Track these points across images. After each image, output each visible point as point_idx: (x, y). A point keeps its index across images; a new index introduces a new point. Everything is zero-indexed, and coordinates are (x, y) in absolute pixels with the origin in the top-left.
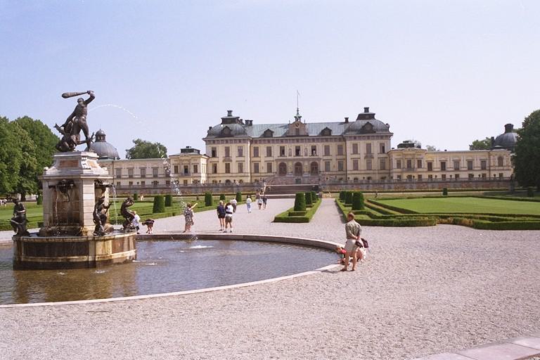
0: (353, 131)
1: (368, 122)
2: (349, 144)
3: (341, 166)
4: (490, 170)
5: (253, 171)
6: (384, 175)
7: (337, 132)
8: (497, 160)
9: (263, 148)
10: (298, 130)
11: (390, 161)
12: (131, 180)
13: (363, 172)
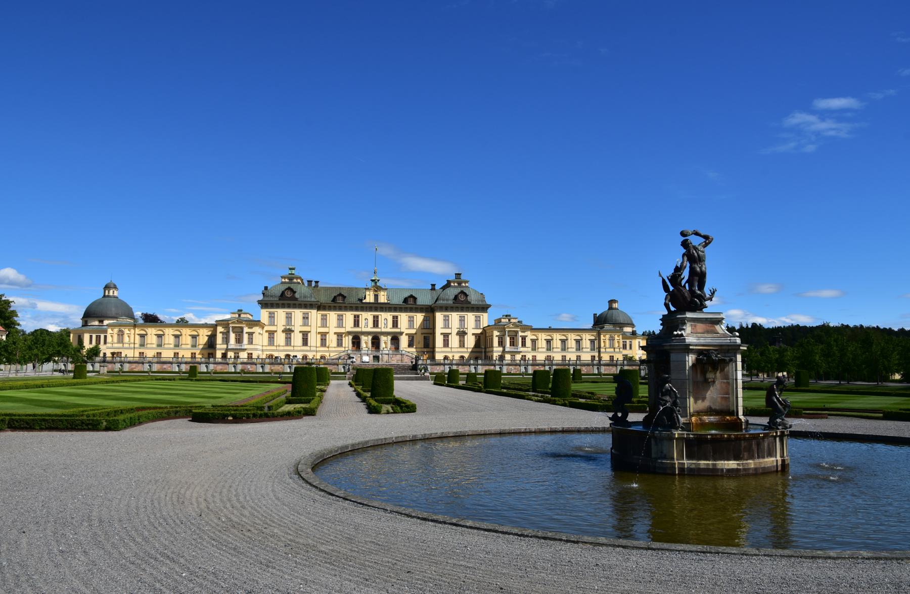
0: (443, 300)
1: (462, 292)
2: (439, 316)
4: (599, 352)
5: (319, 344)
6: (478, 354)
7: (425, 299)
8: (607, 342)
9: (332, 316)
10: (376, 297)
12: (159, 351)
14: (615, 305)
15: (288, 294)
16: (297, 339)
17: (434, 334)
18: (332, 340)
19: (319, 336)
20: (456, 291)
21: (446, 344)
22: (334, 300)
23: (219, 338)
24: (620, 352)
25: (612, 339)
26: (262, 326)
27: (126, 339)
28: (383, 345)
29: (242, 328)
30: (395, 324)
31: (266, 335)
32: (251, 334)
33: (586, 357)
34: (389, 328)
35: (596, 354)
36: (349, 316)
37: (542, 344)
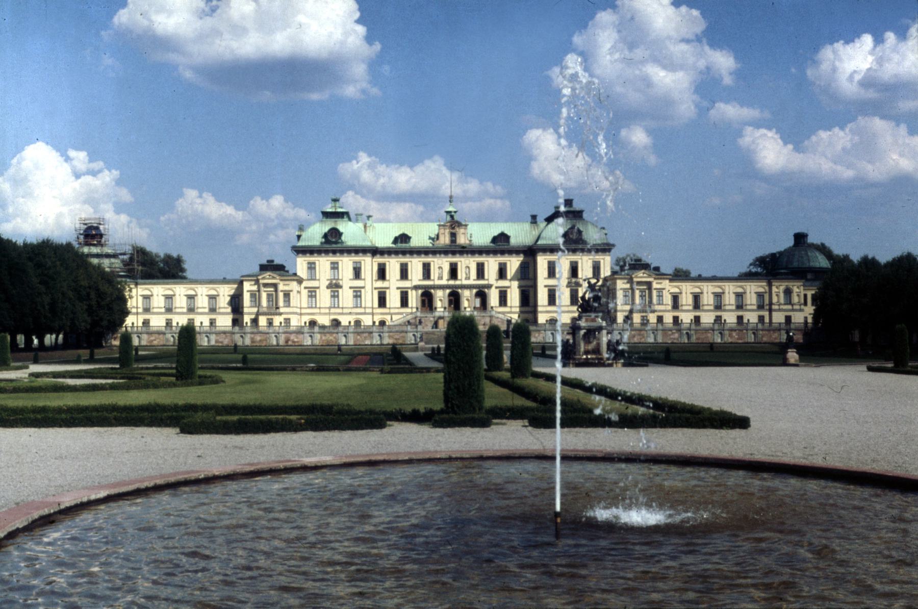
2: (542, 262)
3: (528, 299)
4: (770, 311)
5: (376, 304)
8: (782, 295)
9: (393, 265)
11: (611, 293)
13: (566, 309)
17: (535, 286)
19: (376, 293)
21: (552, 300)
23: (247, 297)
24: (801, 310)
25: (788, 292)
26: (300, 281)
29: (275, 286)
30: (481, 273)
31: (305, 293)
32: (287, 295)
36: (416, 265)
37: (686, 300)
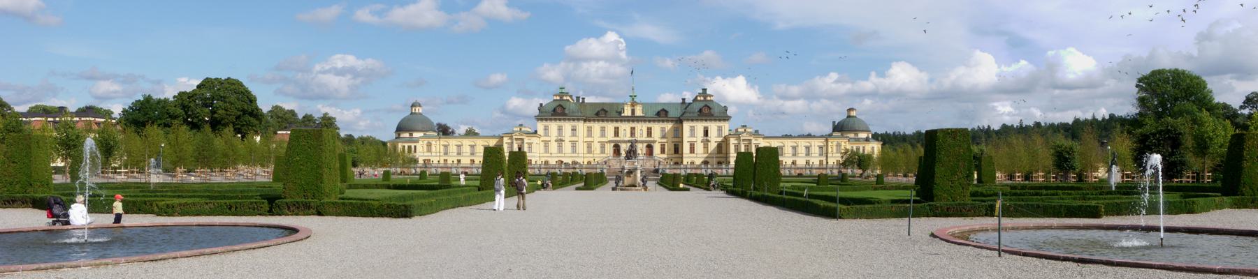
2: (686, 126)
3: (677, 149)
7: (674, 113)
9: (597, 127)
10: (633, 111)
11: (728, 145)
14: (853, 113)
15: (559, 110)
16: (567, 147)
18: (596, 147)
20: (702, 105)
21: (692, 150)
22: (597, 114)
27: (433, 149)
28: (639, 151)
31: (542, 144)
32: (530, 144)
33: (815, 161)
34: (645, 138)
35: (824, 159)
36: (610, 127)
